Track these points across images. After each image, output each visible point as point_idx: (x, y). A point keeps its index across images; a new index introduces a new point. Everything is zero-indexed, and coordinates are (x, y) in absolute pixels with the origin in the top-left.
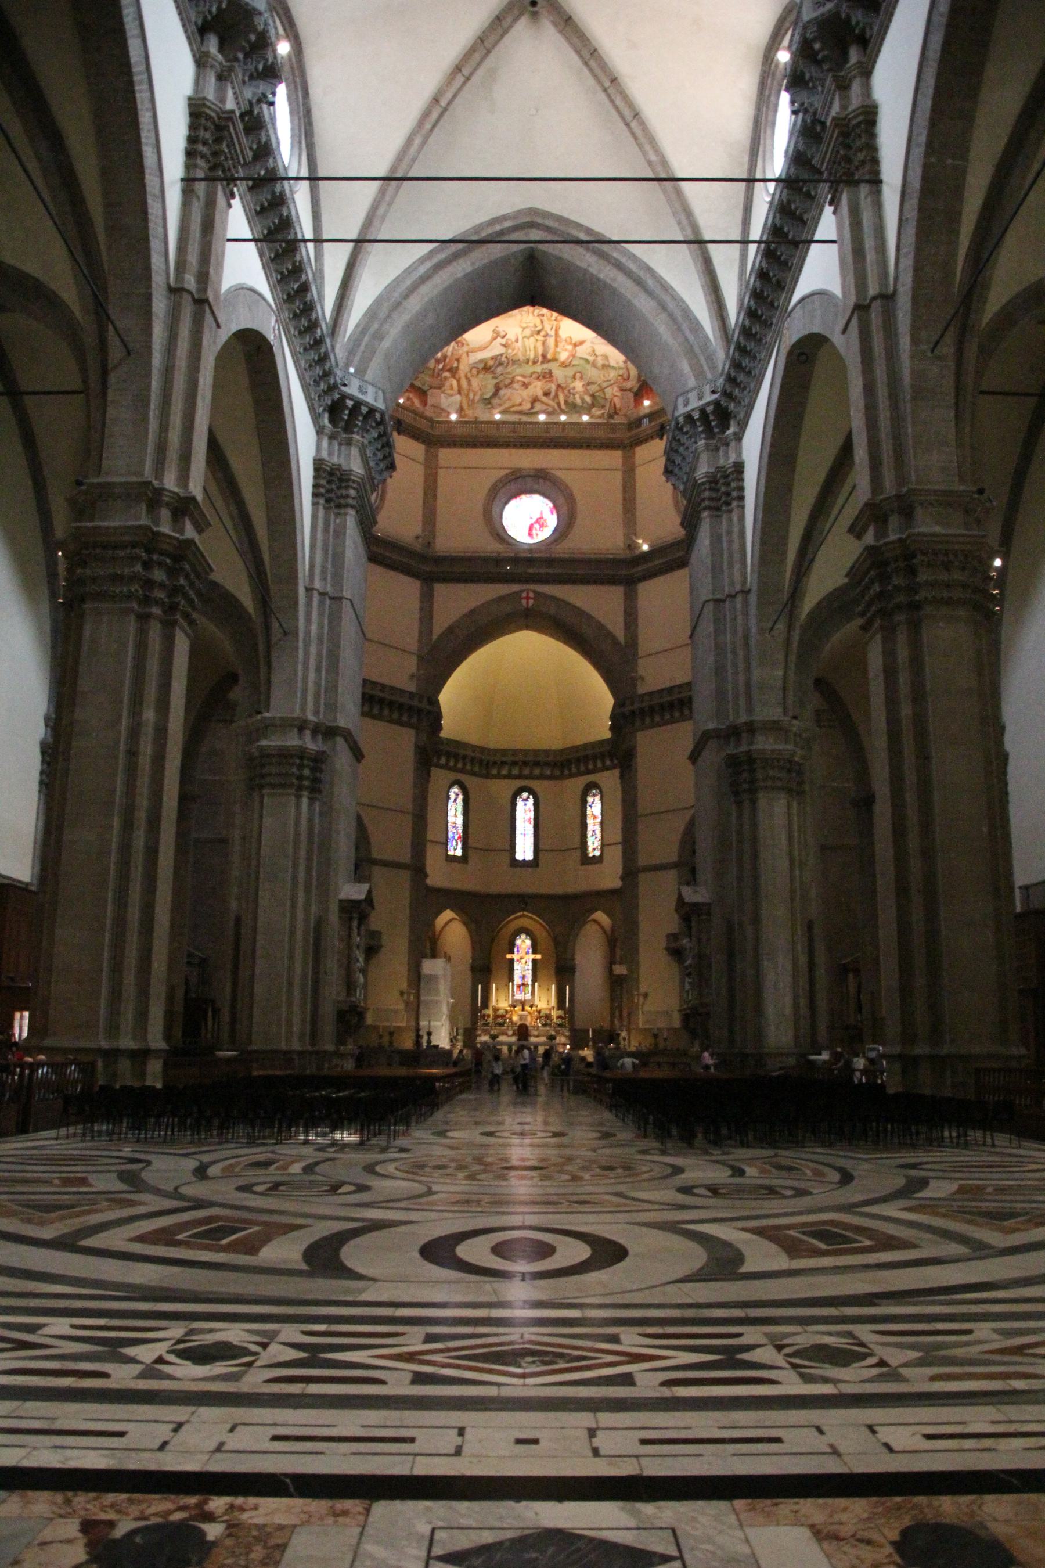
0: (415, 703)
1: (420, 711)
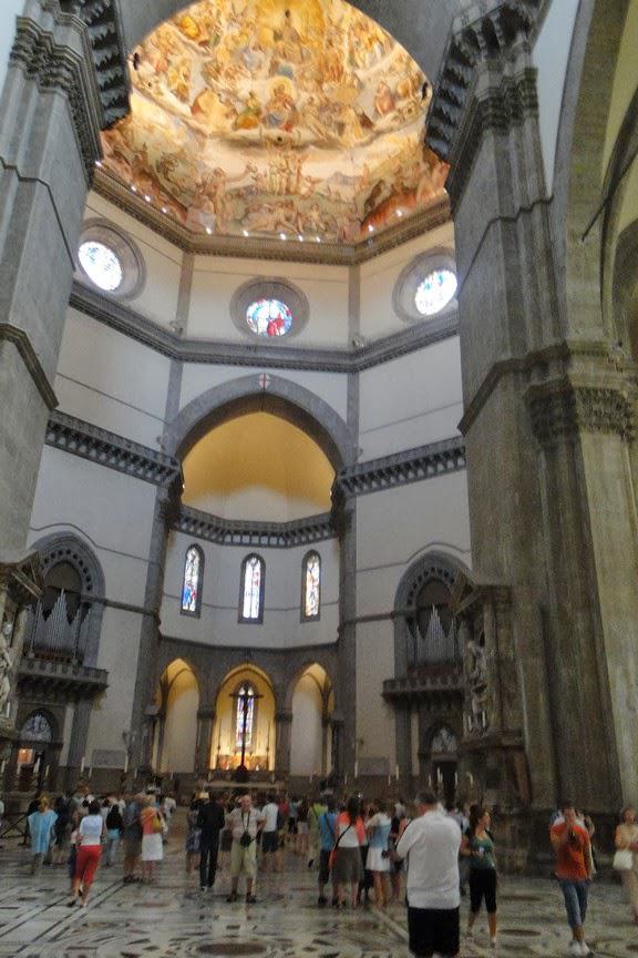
0: (159, 461)
1: (163, 469)
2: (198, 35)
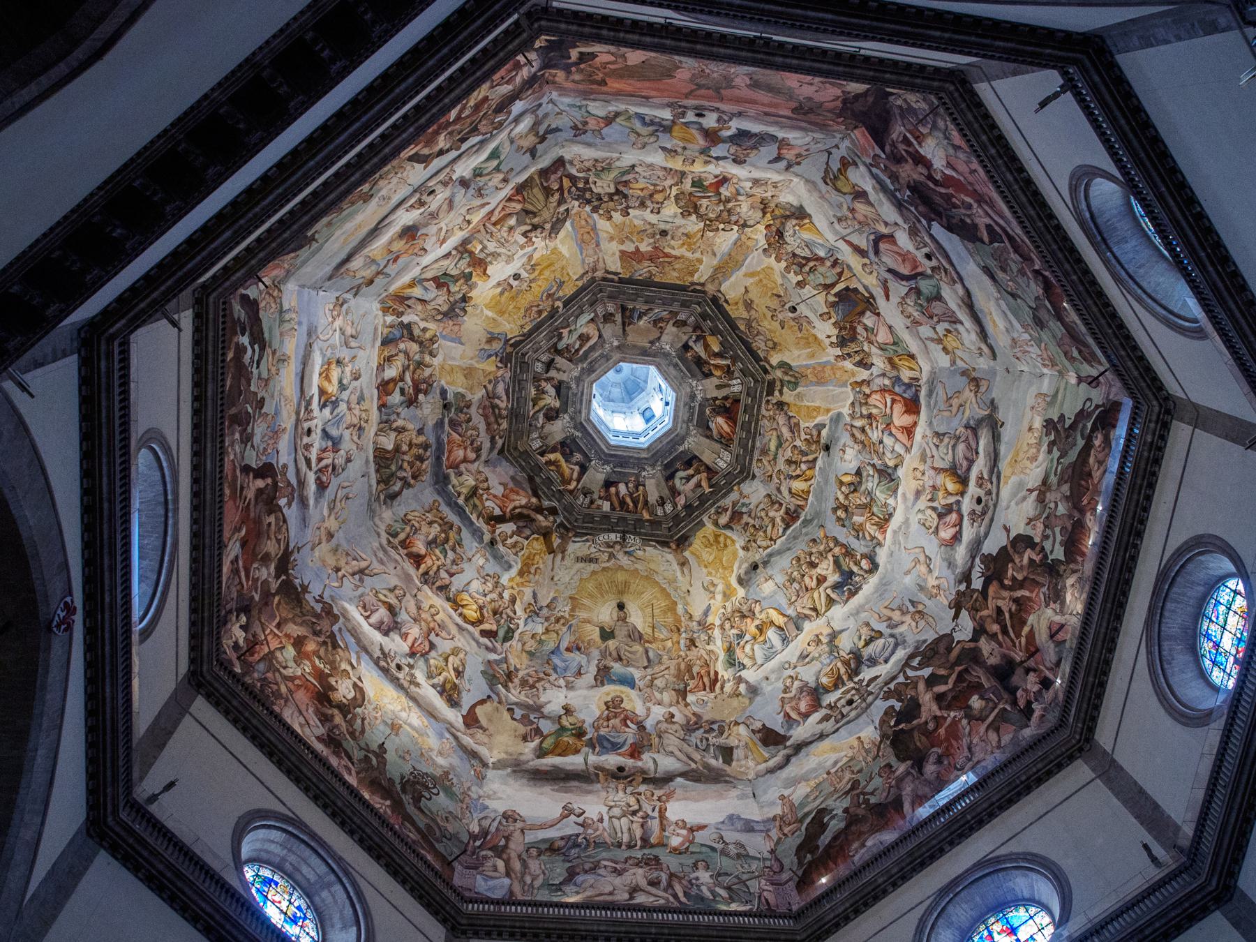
2: (480, 621)
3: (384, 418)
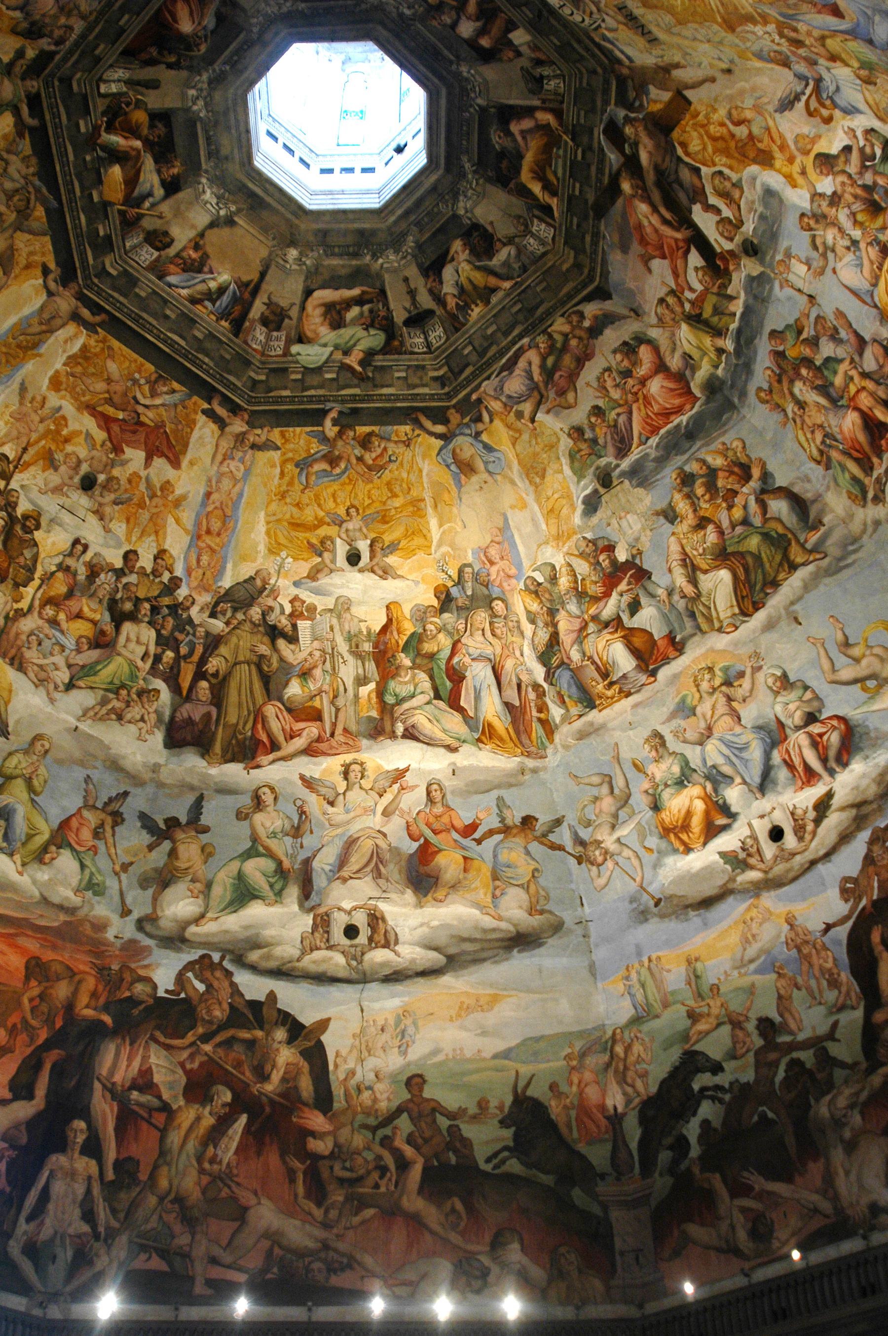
3: (689, 624)
